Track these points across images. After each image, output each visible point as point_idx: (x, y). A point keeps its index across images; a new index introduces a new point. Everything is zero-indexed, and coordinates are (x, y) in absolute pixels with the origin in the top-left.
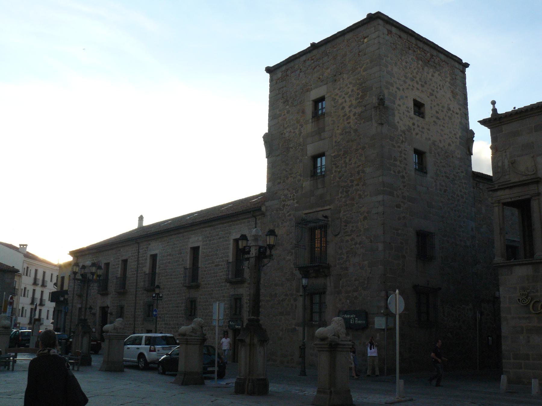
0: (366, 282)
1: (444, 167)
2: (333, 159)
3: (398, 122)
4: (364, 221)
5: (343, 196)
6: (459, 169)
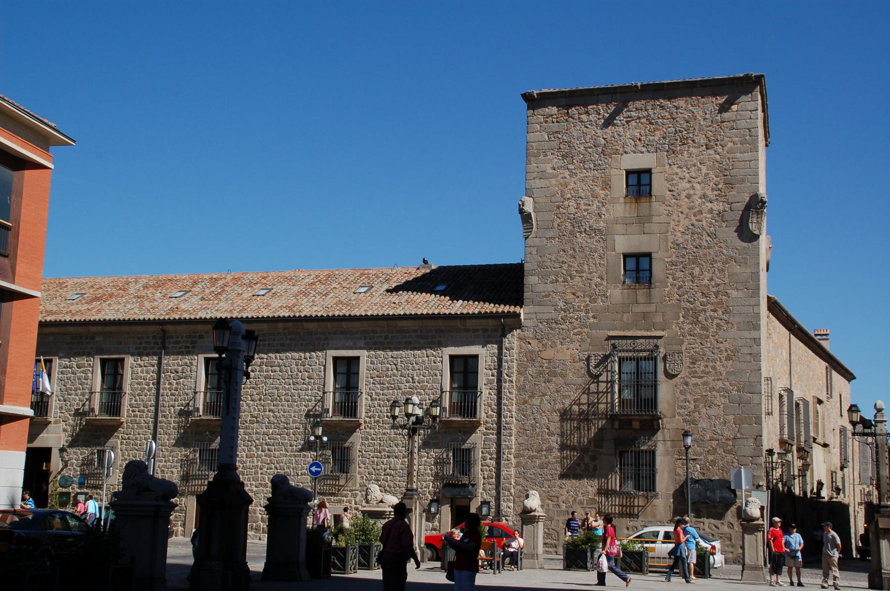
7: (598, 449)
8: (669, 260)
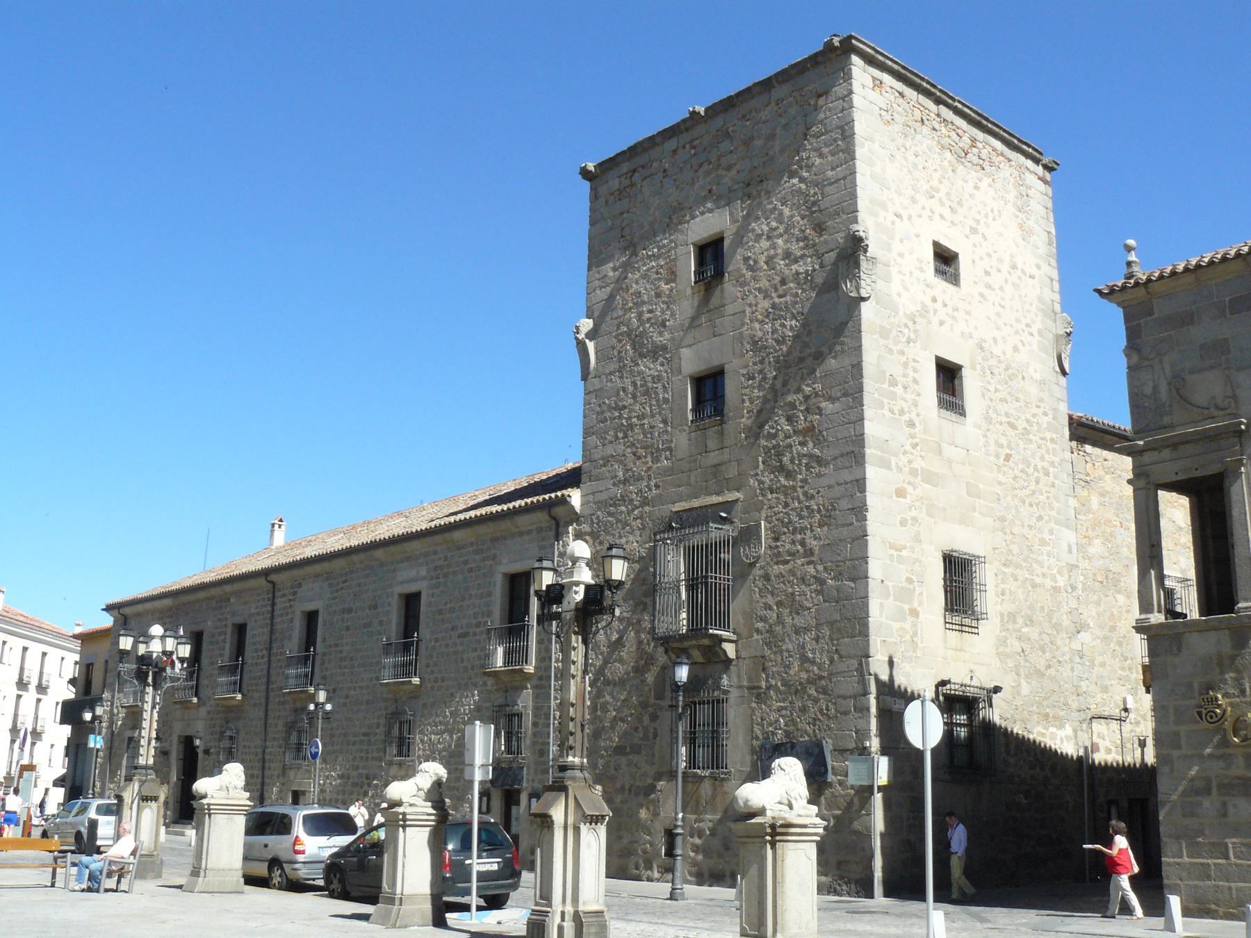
1: (1003, 400)
3: (899, 295)
6: (1038, 407)
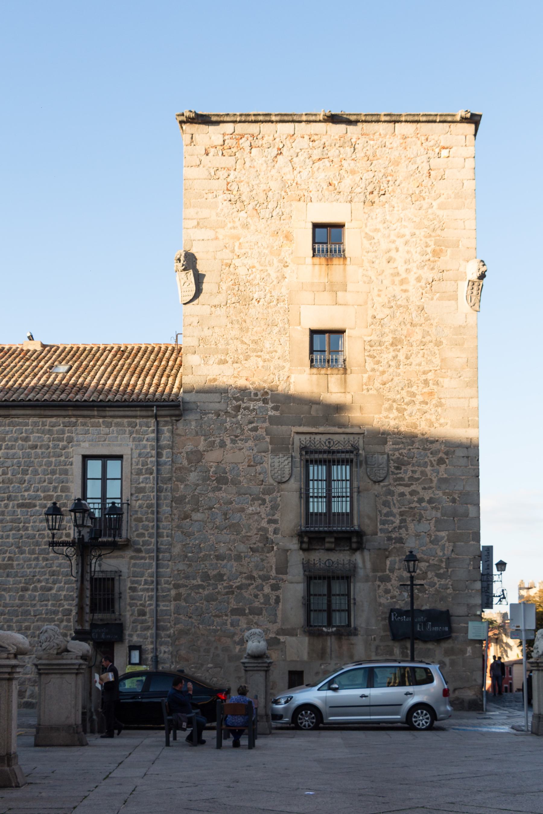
0: (443, 565)
2: (368, 347)
4: (438, 465)
5: (391, 416)
7: (281, 576)
8: (369, 339)
